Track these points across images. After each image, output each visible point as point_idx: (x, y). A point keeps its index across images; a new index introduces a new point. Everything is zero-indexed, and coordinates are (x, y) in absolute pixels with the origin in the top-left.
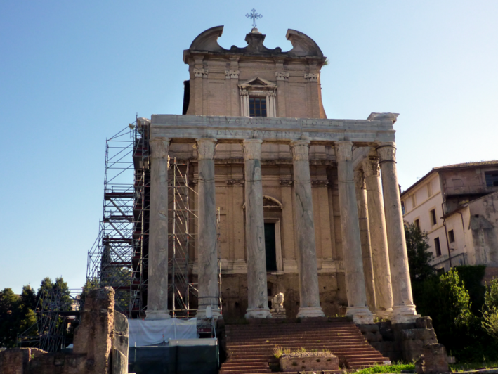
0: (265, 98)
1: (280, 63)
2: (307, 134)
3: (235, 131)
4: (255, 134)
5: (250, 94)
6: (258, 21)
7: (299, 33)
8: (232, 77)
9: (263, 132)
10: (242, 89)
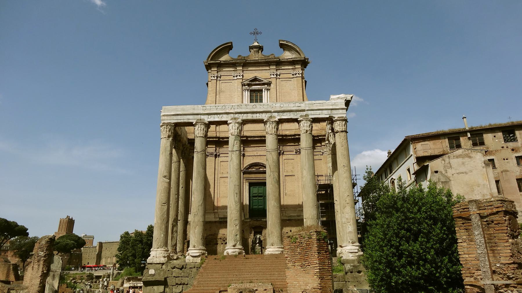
0: (262, 91)
2: (276, 114)
6: (258, 36)
7: (287, 42)
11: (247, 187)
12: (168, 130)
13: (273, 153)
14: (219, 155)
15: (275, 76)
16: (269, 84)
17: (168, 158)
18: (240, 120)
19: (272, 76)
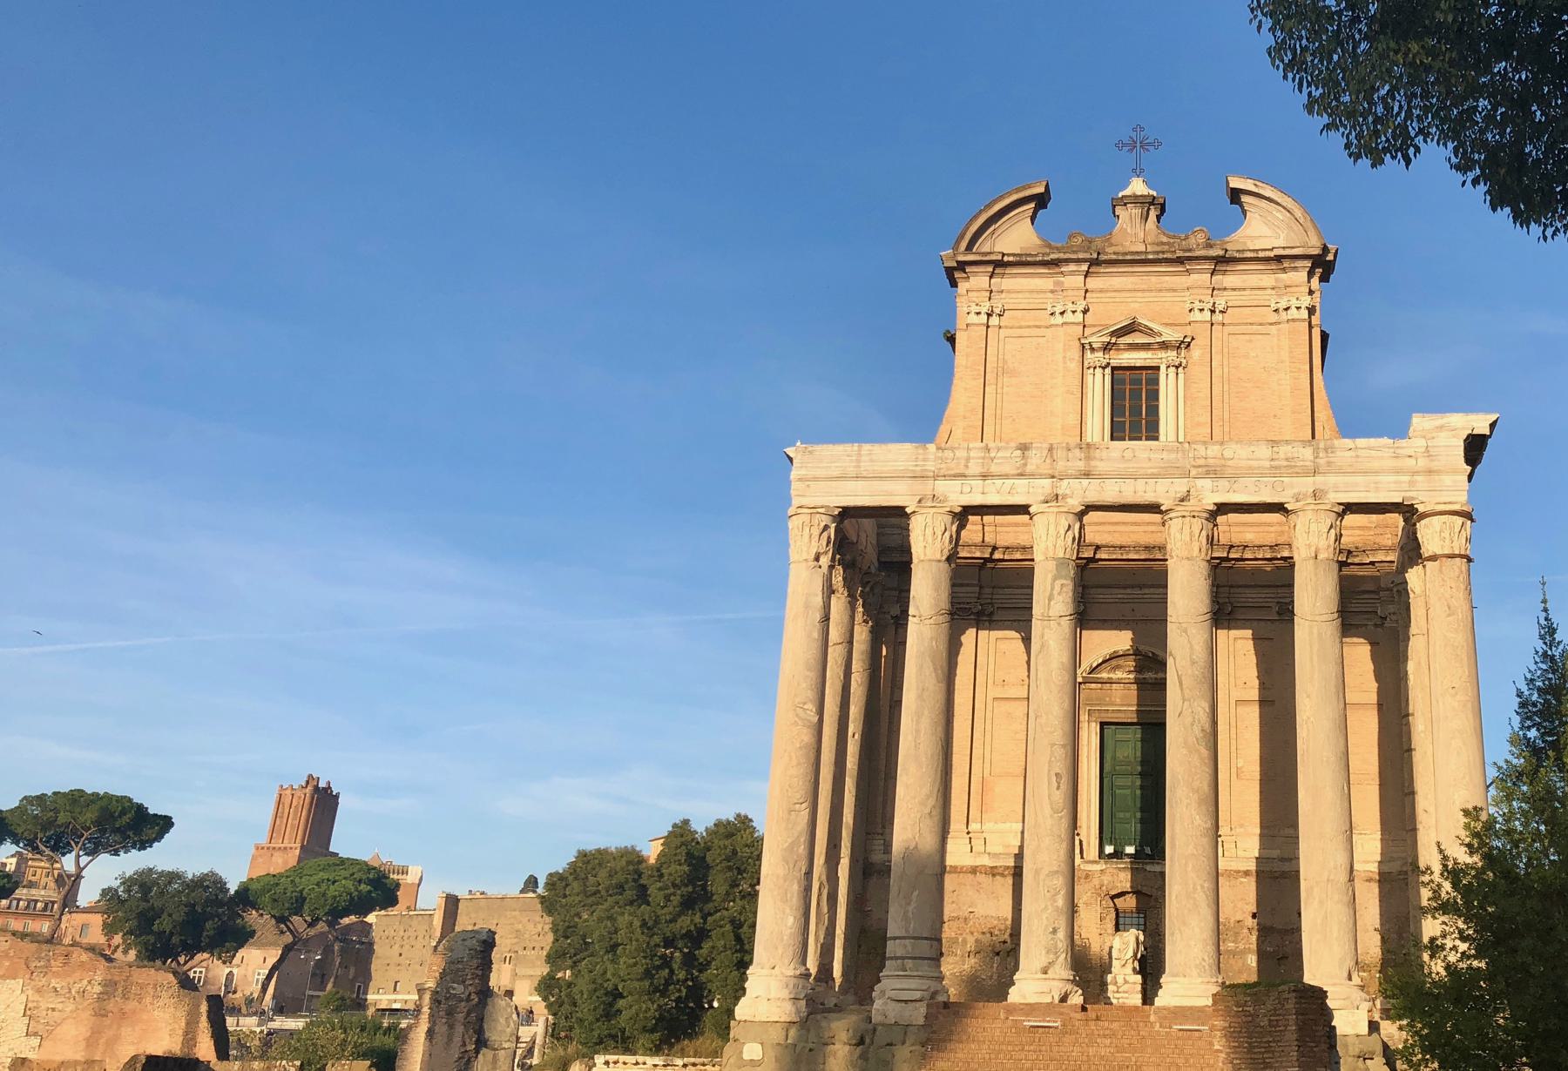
0: (1158, 368)
1: (1200, 272)
3: (1009, 482)
4: (1063, 487)
5: (1114, 363)
8: (1069, 317)
9: (1085, 482)
10: (1092, 350)
11: (1095, 741)
12: (816, 532)
13: (1193, 631)
14: (992, 613)
15: (1207, 315)
16: (1183, 345)
17: (816, 635)
18: (1076, 504)
19: (1197, 316)
